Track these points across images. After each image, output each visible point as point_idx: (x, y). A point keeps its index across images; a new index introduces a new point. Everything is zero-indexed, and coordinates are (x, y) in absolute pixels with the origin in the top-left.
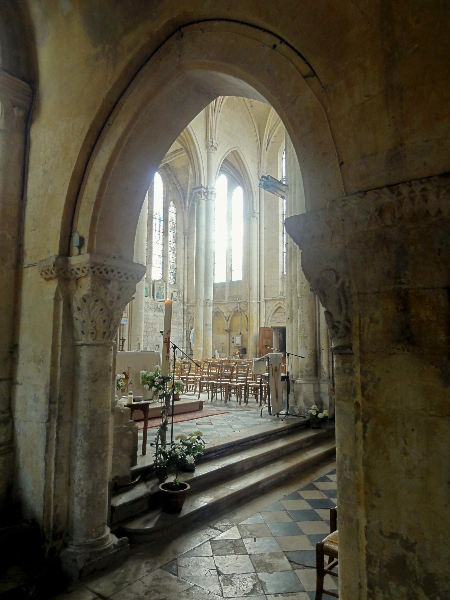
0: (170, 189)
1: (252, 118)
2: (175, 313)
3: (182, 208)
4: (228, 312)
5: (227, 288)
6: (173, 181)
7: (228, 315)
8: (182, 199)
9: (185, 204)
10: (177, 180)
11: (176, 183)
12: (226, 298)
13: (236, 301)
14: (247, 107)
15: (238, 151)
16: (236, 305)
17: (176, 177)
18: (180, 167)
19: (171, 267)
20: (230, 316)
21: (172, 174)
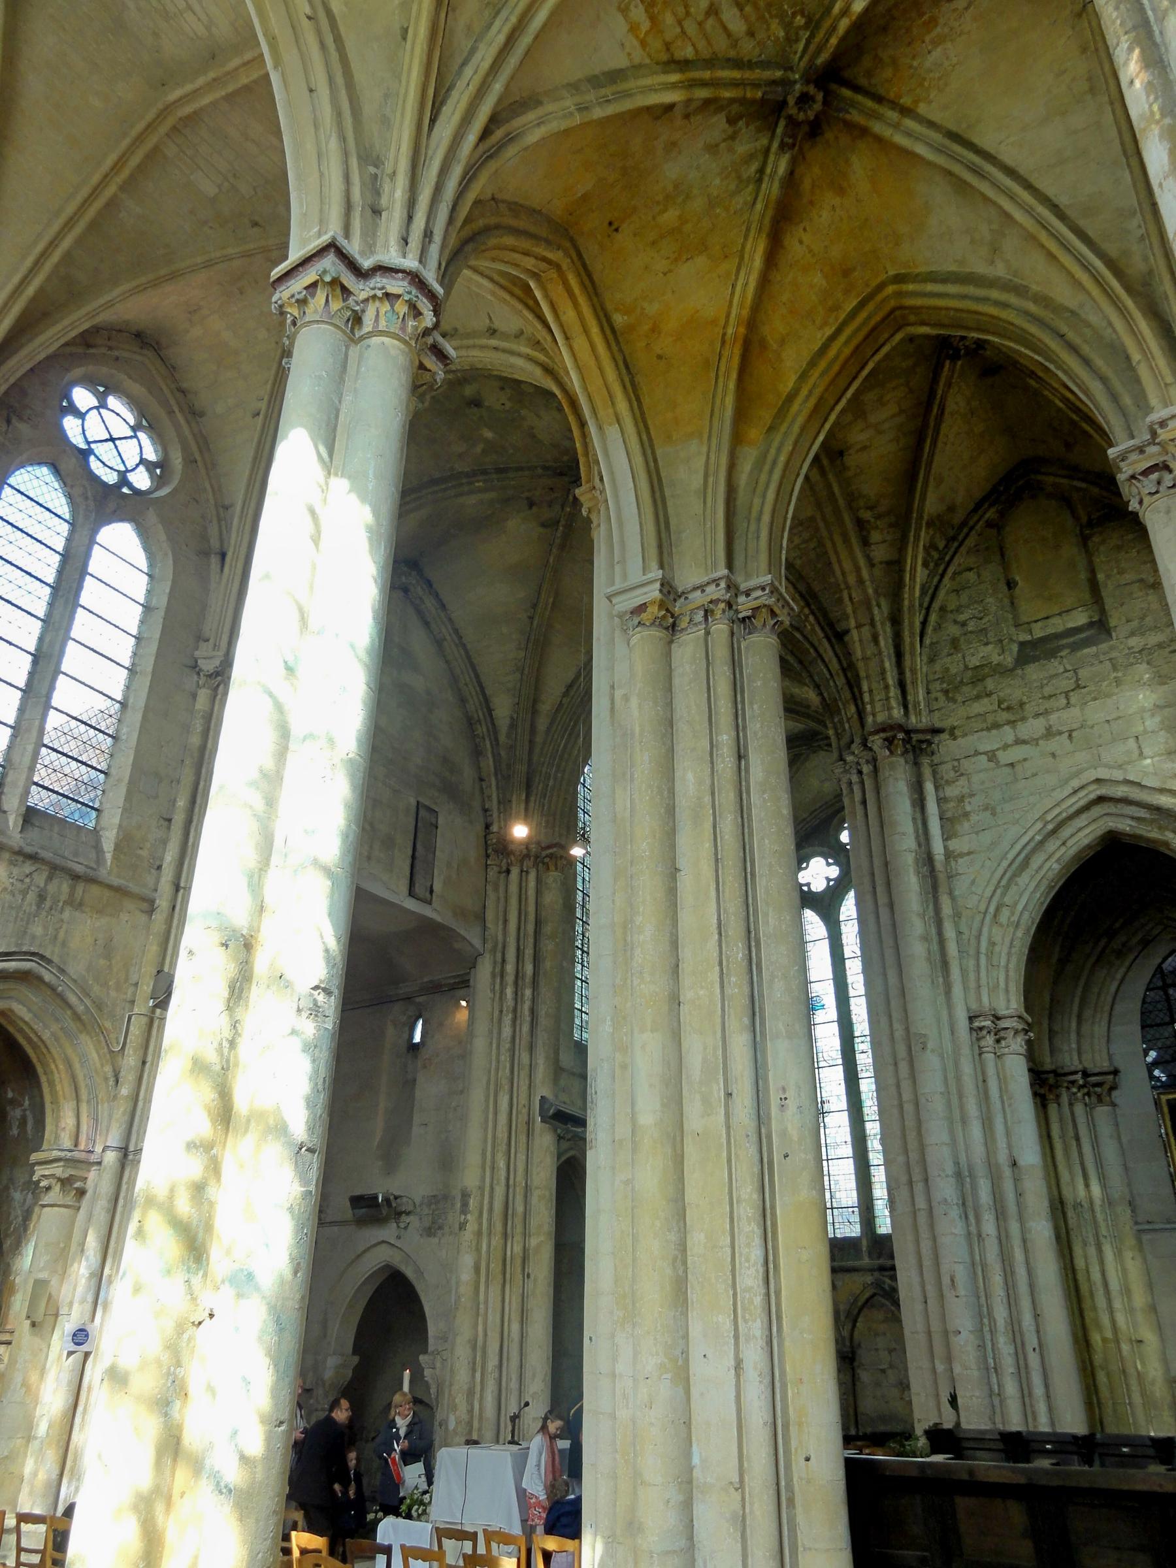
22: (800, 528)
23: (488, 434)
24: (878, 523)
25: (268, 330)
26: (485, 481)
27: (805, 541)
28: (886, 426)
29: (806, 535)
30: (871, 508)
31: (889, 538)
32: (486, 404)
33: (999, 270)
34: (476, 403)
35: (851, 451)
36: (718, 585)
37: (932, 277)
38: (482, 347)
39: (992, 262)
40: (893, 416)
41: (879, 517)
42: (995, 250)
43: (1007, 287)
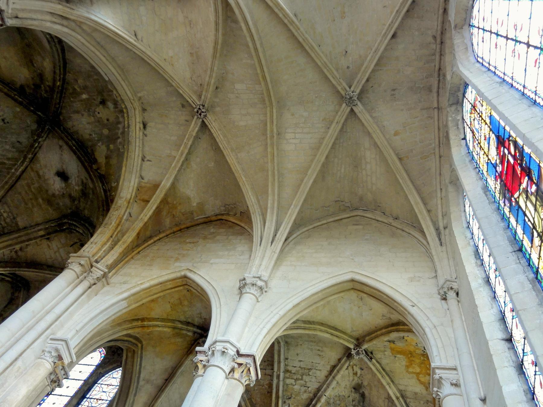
22: (12, 217)
23: (84, 96)
24: (13, 252)
25: (172, 57)
26: (59, 86)
27: (5, 220)
28: (57, 254)
29: (8, 220)
30: (21, 249)
31: (6, 257)
32: (101, 106)
33: (141, 383)
34: (103, 102)
35: (48, 242)
36: (64, 375)
37: (141, 358)
38: (139, 156)
39: (144, 380)
40: (62, 257)
41: (16, 252)
42: (148, 381)
43: (137, 387)
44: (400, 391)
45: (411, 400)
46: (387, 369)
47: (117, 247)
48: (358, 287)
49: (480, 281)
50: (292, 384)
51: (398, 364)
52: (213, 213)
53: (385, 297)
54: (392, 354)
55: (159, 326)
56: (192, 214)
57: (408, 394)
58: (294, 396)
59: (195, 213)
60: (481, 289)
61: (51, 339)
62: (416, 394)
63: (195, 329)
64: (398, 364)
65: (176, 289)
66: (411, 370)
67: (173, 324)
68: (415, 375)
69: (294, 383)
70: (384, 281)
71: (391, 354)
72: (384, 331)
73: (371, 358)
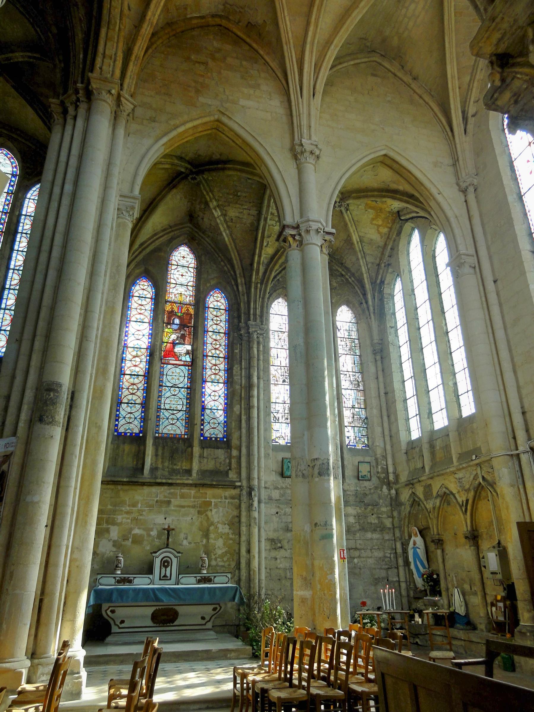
0: (335, 284)
1: (421, 97)
2: (370, 507)
3: (363, 311)
4: (462, 490)
5: (453, 436)
6: (339, 271)
7: (464, 499)
8: (361, 296)
9: (367, 302)
10: (346, 267)
11: (343, 273)
12: (455, 460)
13: (471, 463)
14: (405, 83)
15: (392, 154)
16: (474, 473)
17: (342, 264)
18: (342, 244)
19: (354, 417)
20: (467, 501)
21: (334, 261)
44: (360, 237)
45: (366, 244)
46: (355, 219)
47: (131, 65)
48: (388, 162)
49: (515, 196)
50: (273, 225)
51: (366, 216)
52: (208, 12)
53: (414, 178)
54: (365, 208)
55: (162, 164)
56: (186, 9)
57: (365, 240)
58: (273, 235)
59: (189, 9)
60: (516, 204)
61: (121, 196)
62: (371, 240)
63: (187, 165)
64: (366, 216)
65: (205, 133)
66: (374, 222)
67: (172, 161)
68: (376, 227)
69: (275, 225)
70: (415, 163)
71: (363, 208)
72: (376, 193)
73: (347, 210)
